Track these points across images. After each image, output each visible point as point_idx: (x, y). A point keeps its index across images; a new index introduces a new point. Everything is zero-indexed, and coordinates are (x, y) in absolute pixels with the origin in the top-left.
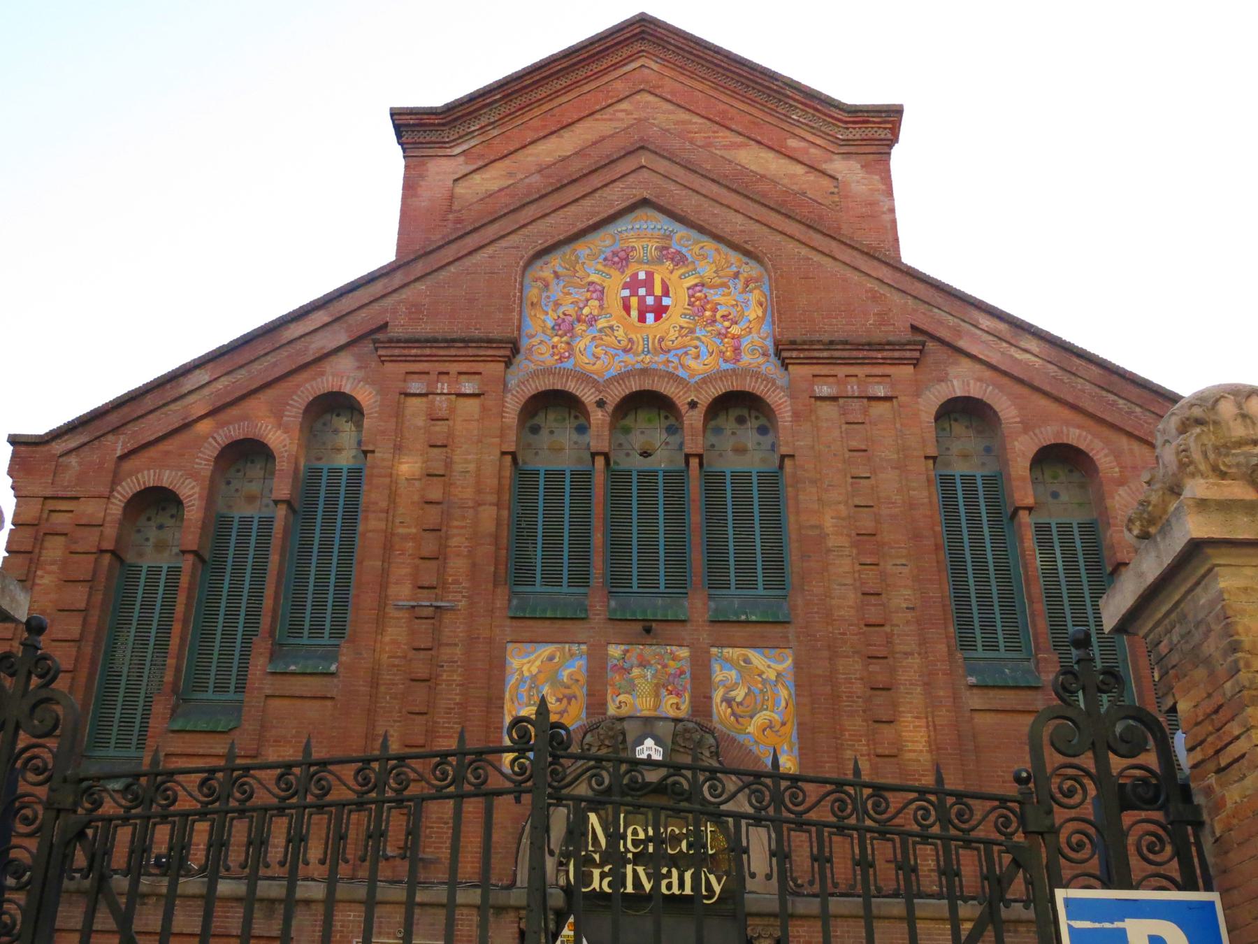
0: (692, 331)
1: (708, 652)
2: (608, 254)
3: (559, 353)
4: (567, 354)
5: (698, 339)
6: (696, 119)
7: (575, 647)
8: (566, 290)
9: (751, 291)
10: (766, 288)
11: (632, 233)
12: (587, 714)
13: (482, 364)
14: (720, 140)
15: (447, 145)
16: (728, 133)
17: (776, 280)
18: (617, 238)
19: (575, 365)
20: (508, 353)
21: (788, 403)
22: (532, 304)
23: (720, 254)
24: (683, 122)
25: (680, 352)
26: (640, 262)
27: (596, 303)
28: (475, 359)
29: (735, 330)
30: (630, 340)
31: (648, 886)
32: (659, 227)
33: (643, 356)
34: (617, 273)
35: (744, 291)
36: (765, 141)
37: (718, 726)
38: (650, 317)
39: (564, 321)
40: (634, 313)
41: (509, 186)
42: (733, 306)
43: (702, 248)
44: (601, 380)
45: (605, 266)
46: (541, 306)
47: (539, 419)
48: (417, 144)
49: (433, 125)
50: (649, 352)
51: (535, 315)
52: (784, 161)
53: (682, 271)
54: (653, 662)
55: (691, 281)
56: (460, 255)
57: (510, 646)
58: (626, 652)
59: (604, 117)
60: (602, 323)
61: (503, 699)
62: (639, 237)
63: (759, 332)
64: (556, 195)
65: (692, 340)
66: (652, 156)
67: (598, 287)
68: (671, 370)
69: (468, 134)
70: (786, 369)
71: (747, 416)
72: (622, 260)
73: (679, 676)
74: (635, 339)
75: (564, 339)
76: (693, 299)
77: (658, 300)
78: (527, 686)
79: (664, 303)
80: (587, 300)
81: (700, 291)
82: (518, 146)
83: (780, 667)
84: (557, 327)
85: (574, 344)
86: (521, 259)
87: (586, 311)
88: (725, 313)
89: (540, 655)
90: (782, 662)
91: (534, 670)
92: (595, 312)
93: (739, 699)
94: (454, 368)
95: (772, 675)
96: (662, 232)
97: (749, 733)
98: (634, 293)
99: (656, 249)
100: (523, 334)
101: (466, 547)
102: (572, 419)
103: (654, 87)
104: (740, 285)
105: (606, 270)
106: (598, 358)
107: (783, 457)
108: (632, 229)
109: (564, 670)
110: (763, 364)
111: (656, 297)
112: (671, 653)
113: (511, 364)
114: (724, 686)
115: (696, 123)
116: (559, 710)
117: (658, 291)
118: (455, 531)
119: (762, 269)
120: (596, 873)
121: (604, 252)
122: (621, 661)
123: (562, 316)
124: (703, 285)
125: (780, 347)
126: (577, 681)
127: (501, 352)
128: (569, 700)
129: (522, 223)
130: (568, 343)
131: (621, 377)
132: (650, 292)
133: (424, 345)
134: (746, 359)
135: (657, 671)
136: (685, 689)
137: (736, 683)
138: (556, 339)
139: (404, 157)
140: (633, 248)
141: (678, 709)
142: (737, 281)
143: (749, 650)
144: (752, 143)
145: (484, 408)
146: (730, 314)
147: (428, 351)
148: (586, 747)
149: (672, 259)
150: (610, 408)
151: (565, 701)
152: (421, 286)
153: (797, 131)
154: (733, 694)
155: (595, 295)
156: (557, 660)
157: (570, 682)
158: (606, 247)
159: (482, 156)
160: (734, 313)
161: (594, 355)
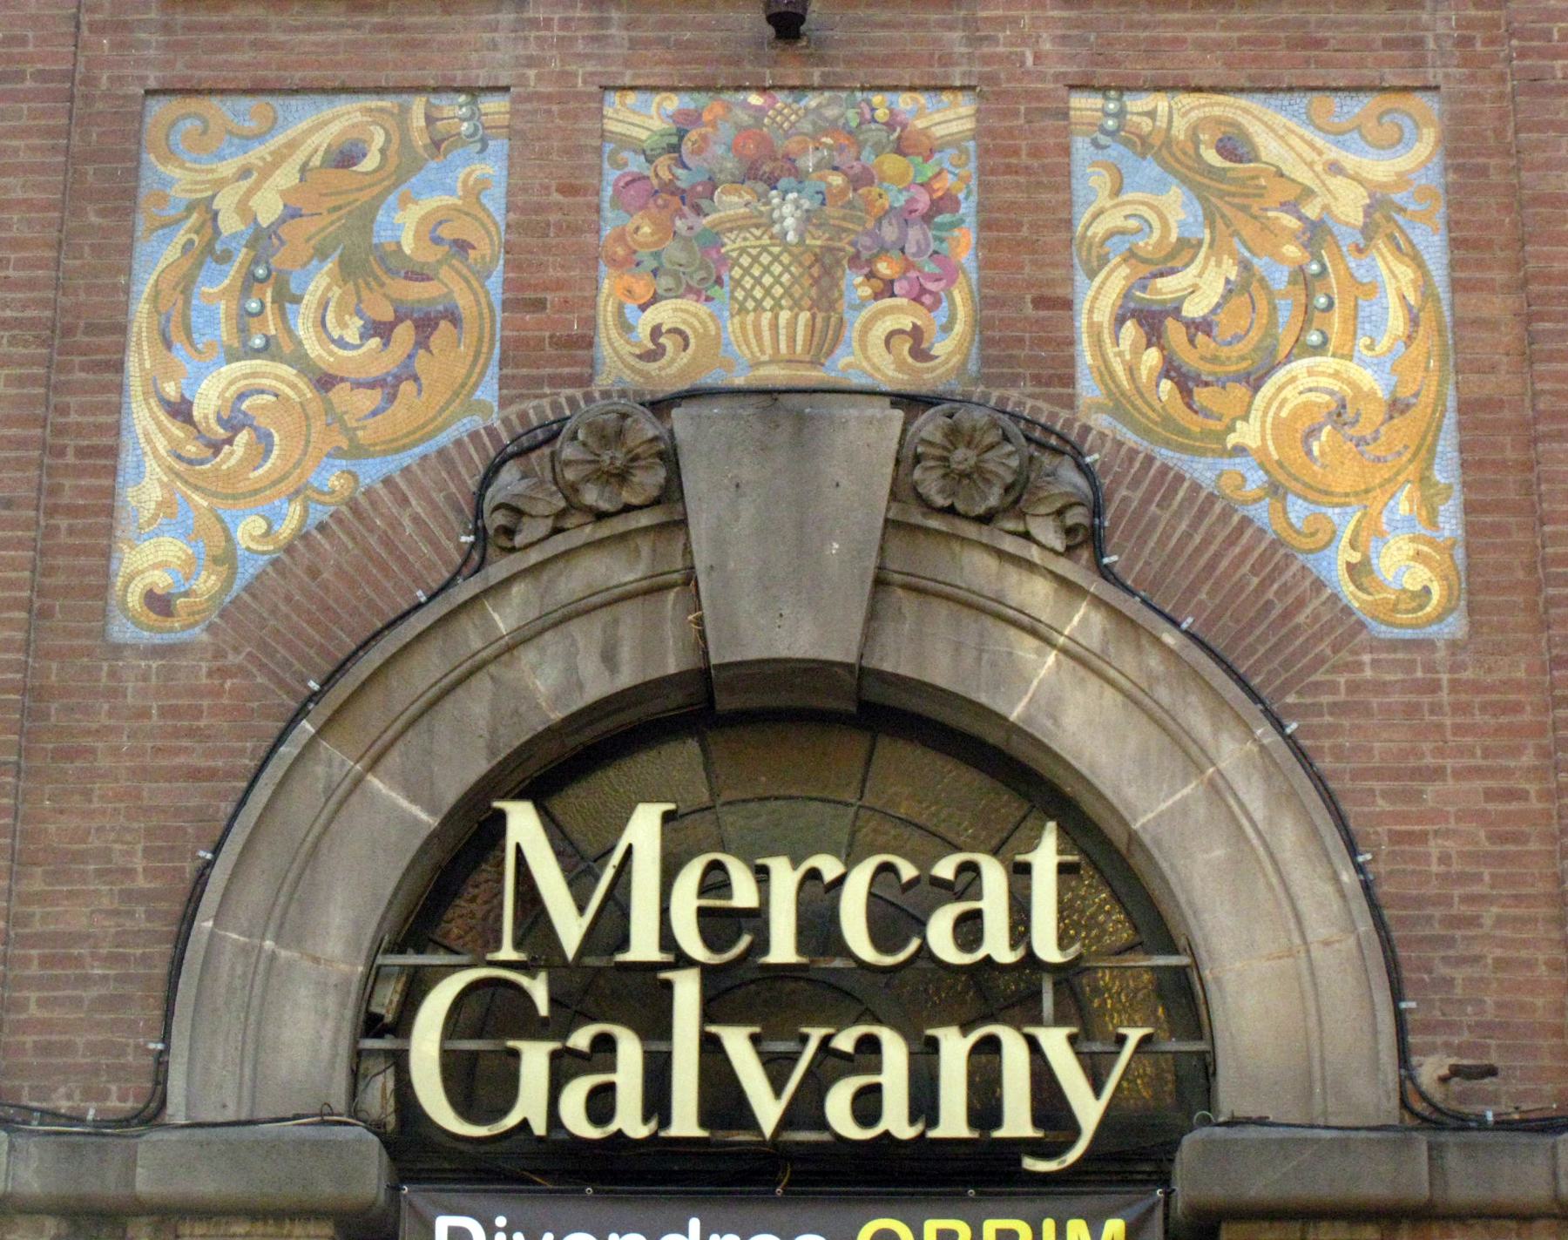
1: (1064, 114)
7: (454, 108)
12: (504, 382)
31: (768, 1110)
37: (1101, 422)
54: (809, 162)
57: (158, 109)
58: (684, 124)
61: (122, 329)
73: (927, 218)
78: (231, 274)
83: (1381, 168)
89: (292, 145)
90: (1395, 143)
91: (268, 208)
93: (1193, 310)
95: (1348, 205)
97: (1240, 450)
109: (404, 202)
112: (890, 125)
114: (1131, 255)
116: (375, 371)
120: (535, 1058)
122: (664, 161)
126: (462, 246)
128: (426, 325)
135: (824, 198)
136: (950, 273)
137: (1183, 243)
141: (920, 353)
143: (1243, 101)
148: (500, 519)
151: (404, 334)
154: (1168, 287)
156: (370, 163)
157: (431, 255)
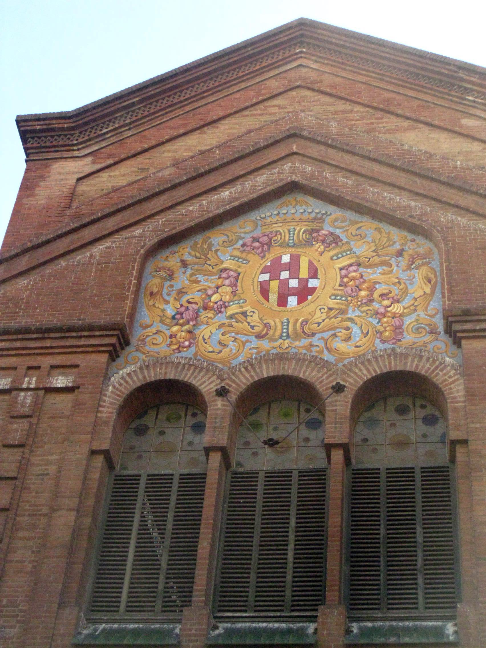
0: (343, 312)
2: (248, 239)
3: (179, 342)
4: (187, 343)
5: (351, 320)
6: (357, 108)
8: (193, 278)
9: (417, 268)
10: (435, 264)
11: (277, 218)
13: (81, 356)
14: (385, 125)
15: (75, 148)
16: (393, 118)
17: (447, 252)
18: (260, 223)
19: (195, 355)
20: (113, 340)
21: (462, 381)
22: (151, 294)
23: (380, 233)
24: (344, 112)
25: (326, 335)
26: (285, 245)
27: (229, 289)
28: (74, 350)
29: (397, 308)
30: (267, 325)
32: (310, 211)
33: (281, 341)
34: (257, 258)
35: (409, 268)
36: (436, 122)
38: (292, 301)
39: (187, 309)
40: (273, 297)
41: (136, 182)
42: (394, 284)
43: (360, 228)
44: (226, 369)
45: (242, 252)
46: (161, 294)
47: (148, 420)
48: (41, 150)
49: (63, 129)
50: (288, 336)
51: (154, 305)
52: (457, 140)
53: (331, 253)
55: (345, 262)
56: (72, 247)
59: (254, 112)
60: (233, 309)
62: (285, 221)
63: (426, 309)
64: (190, 185)
65: (342, 321)
66: (302, 142)
67: (232, 273)
68: (314, 353)
69: (100, 136)
70: (459, 346)
71: (411, 406)
72: (263, 245)
74: (272, 323)
75: (186, 327)
76: (345, 280)
77: (304, 282)
79: (310, 285)
80: (218, 287)
81: (355, 271)
82: (153, 142)
84: (178, 316)
85: (197, 332)
86: (142, 247)
87: (214, 298)
88: (385, 292)
92: (227, 298)
94: (46, 362)
96: (314, 215)
98: (275, 276)
99: (304, 232)
100: (136, 325)
101: (31, 562)
102: (189, 418)
103: (312, 82)
104: (404, 262)
105: (244, 255)
106: (225, 346)
107: (454, 443)
108: (278, 214)
110: (430, 342)
111: (301, 280)
113: (118, 356)
115: (357, 112)
117: (304, 273)
118: (20, 543)
119: (431, 245)
121: (242, 238)
123: (186, 305)
124: (359, 265)
125: (450, 319)
127: (106, 341)
129: (148, 213)
130: (190, 332)
131: (248, 365)
132: (294, 275)
133: (15, 337)
134: (409, 338)
138: (175, 329)
139: (26, 161)
140: (278, 233)
142: (400, 259)
144: (421, 125)
145: (77, 405)
146: (390, 292)
147: (18, 344)
149: (323, 242)
150: (233, 397)
152: (22, 282)
153: (473, 111)
155: (227, 282)
158: (245, 233)
159: (109, 156)
160: (395, 291)
161: (220, 343)
